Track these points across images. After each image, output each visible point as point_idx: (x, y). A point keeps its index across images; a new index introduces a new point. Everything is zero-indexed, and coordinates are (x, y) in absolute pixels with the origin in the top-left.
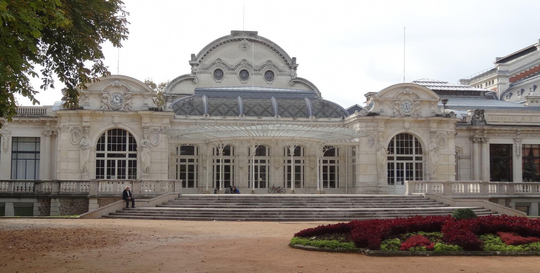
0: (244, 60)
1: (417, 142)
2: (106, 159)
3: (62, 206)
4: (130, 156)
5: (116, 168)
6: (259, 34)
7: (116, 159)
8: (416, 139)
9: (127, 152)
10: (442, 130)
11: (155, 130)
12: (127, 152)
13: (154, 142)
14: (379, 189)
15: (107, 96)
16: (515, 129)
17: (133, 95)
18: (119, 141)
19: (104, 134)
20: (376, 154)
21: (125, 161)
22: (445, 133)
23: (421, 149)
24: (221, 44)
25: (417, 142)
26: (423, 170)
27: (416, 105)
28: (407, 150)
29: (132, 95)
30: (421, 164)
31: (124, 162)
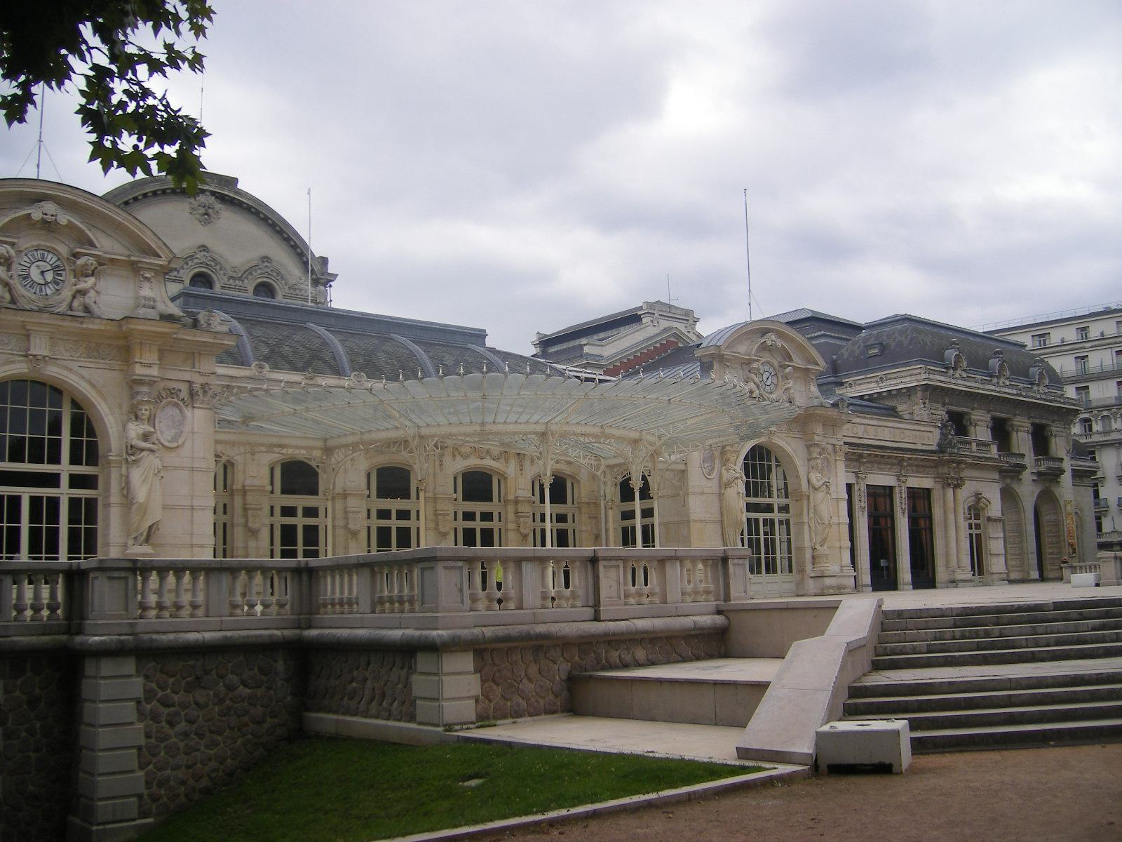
0: (204, 248)
3: (149, 695)
4: (76, 481)
5: (25, 525)
6: (240, 186)
7: (26, 494)
9: (65, 468)
11: (172, 393)
12: (65, 468)
15: (12, 252)
17: (104, 264)
20: (721, 496)
22: (830, 447)
24: (145, 195)
27: (786, 377)
29: (101, 262)
31: (54, 503)
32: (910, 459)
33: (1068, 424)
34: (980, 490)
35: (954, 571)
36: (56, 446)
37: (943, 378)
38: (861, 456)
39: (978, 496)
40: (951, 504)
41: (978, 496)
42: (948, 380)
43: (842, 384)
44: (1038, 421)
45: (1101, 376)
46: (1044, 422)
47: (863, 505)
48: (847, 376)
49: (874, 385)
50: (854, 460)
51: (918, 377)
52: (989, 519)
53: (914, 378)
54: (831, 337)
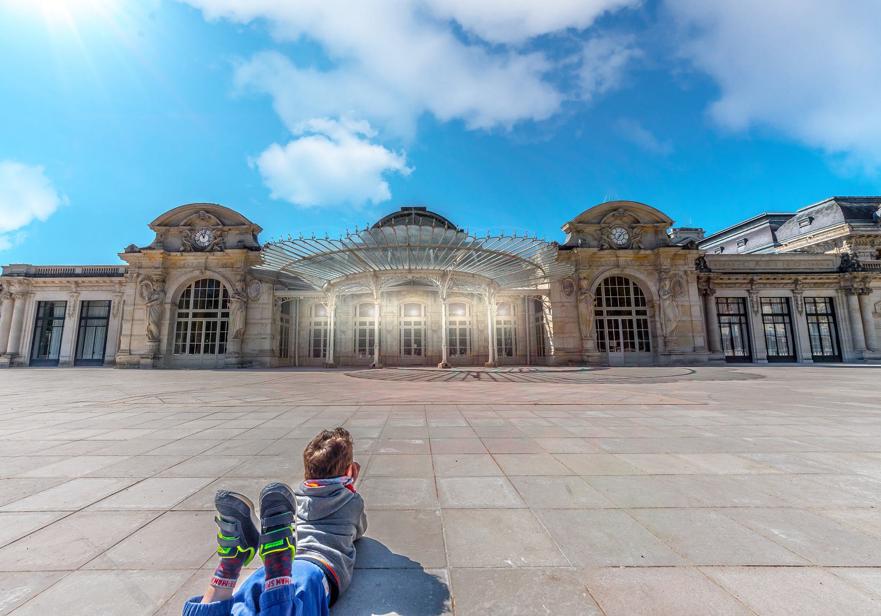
1: (636, 290)
2: (190, 320)
8: (634, 284)
13: (253, 295)
14: (585, 358)
16: (750, 277)
18: (210, 296)
19: (190, 286)
21: (216, 322)
22: (682, 273)
23: (643, 299)
25: (636, 290)
26: (649, 330)
28: (622, 300)
30: (645, 321)
35: (861, 352)
36: (217, 302)
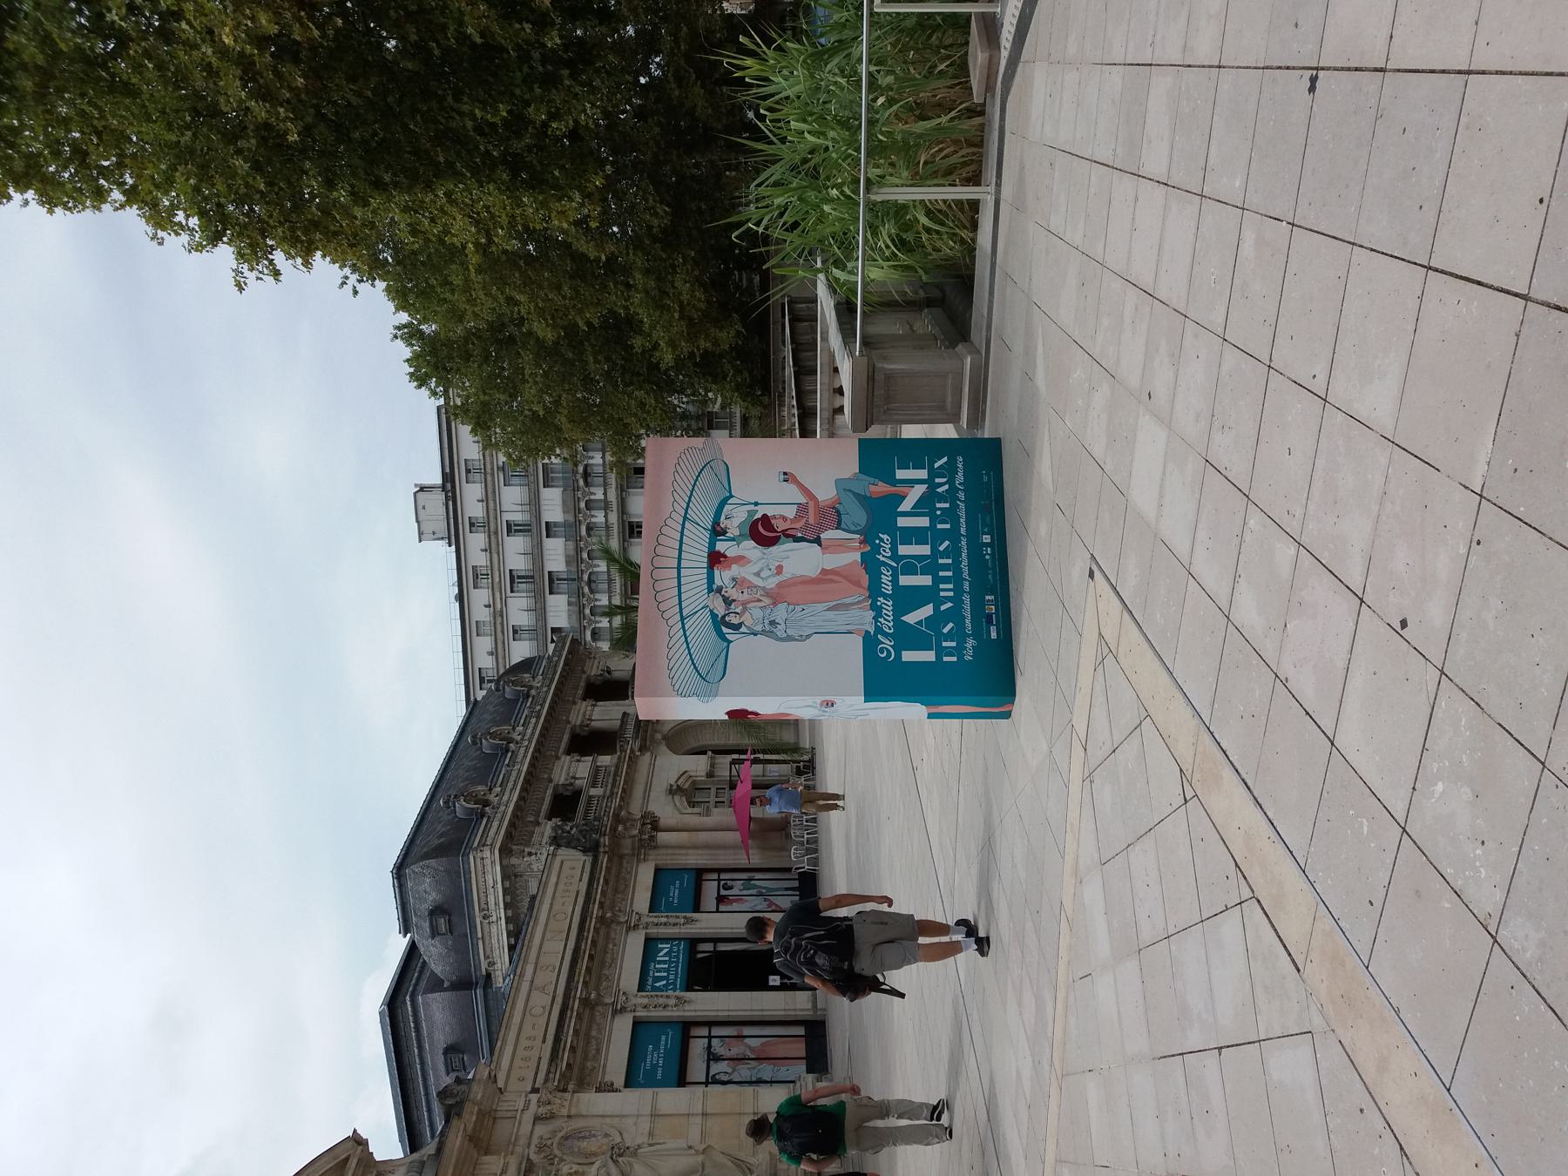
10: (523, 1141)
22: (541, 1130)
32: (601, 905)
33: (590, 654)
34: (665, 786)
37: (496, 824)
38: (585, 1002)
39: (673, 791)
40: (683, 837)
41: (673, 791)
42: (499, 815)
43: (488, 976)
44: (580, 692)
45: (540, 611)
46: (582, 684)
47: (672, 1002)
48: (478, 966)
49: (494, 929)
50: (592, 1017)
51: (488, 862)
52: (710, 775)
53: (489, 868)
54: (417, 984)
